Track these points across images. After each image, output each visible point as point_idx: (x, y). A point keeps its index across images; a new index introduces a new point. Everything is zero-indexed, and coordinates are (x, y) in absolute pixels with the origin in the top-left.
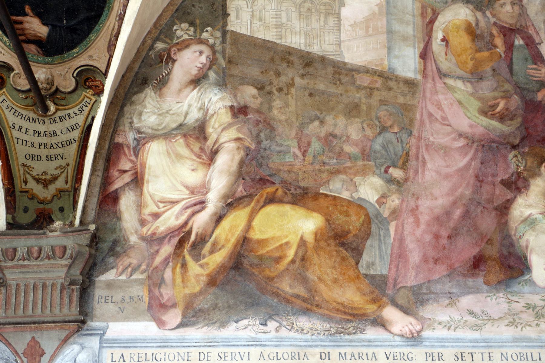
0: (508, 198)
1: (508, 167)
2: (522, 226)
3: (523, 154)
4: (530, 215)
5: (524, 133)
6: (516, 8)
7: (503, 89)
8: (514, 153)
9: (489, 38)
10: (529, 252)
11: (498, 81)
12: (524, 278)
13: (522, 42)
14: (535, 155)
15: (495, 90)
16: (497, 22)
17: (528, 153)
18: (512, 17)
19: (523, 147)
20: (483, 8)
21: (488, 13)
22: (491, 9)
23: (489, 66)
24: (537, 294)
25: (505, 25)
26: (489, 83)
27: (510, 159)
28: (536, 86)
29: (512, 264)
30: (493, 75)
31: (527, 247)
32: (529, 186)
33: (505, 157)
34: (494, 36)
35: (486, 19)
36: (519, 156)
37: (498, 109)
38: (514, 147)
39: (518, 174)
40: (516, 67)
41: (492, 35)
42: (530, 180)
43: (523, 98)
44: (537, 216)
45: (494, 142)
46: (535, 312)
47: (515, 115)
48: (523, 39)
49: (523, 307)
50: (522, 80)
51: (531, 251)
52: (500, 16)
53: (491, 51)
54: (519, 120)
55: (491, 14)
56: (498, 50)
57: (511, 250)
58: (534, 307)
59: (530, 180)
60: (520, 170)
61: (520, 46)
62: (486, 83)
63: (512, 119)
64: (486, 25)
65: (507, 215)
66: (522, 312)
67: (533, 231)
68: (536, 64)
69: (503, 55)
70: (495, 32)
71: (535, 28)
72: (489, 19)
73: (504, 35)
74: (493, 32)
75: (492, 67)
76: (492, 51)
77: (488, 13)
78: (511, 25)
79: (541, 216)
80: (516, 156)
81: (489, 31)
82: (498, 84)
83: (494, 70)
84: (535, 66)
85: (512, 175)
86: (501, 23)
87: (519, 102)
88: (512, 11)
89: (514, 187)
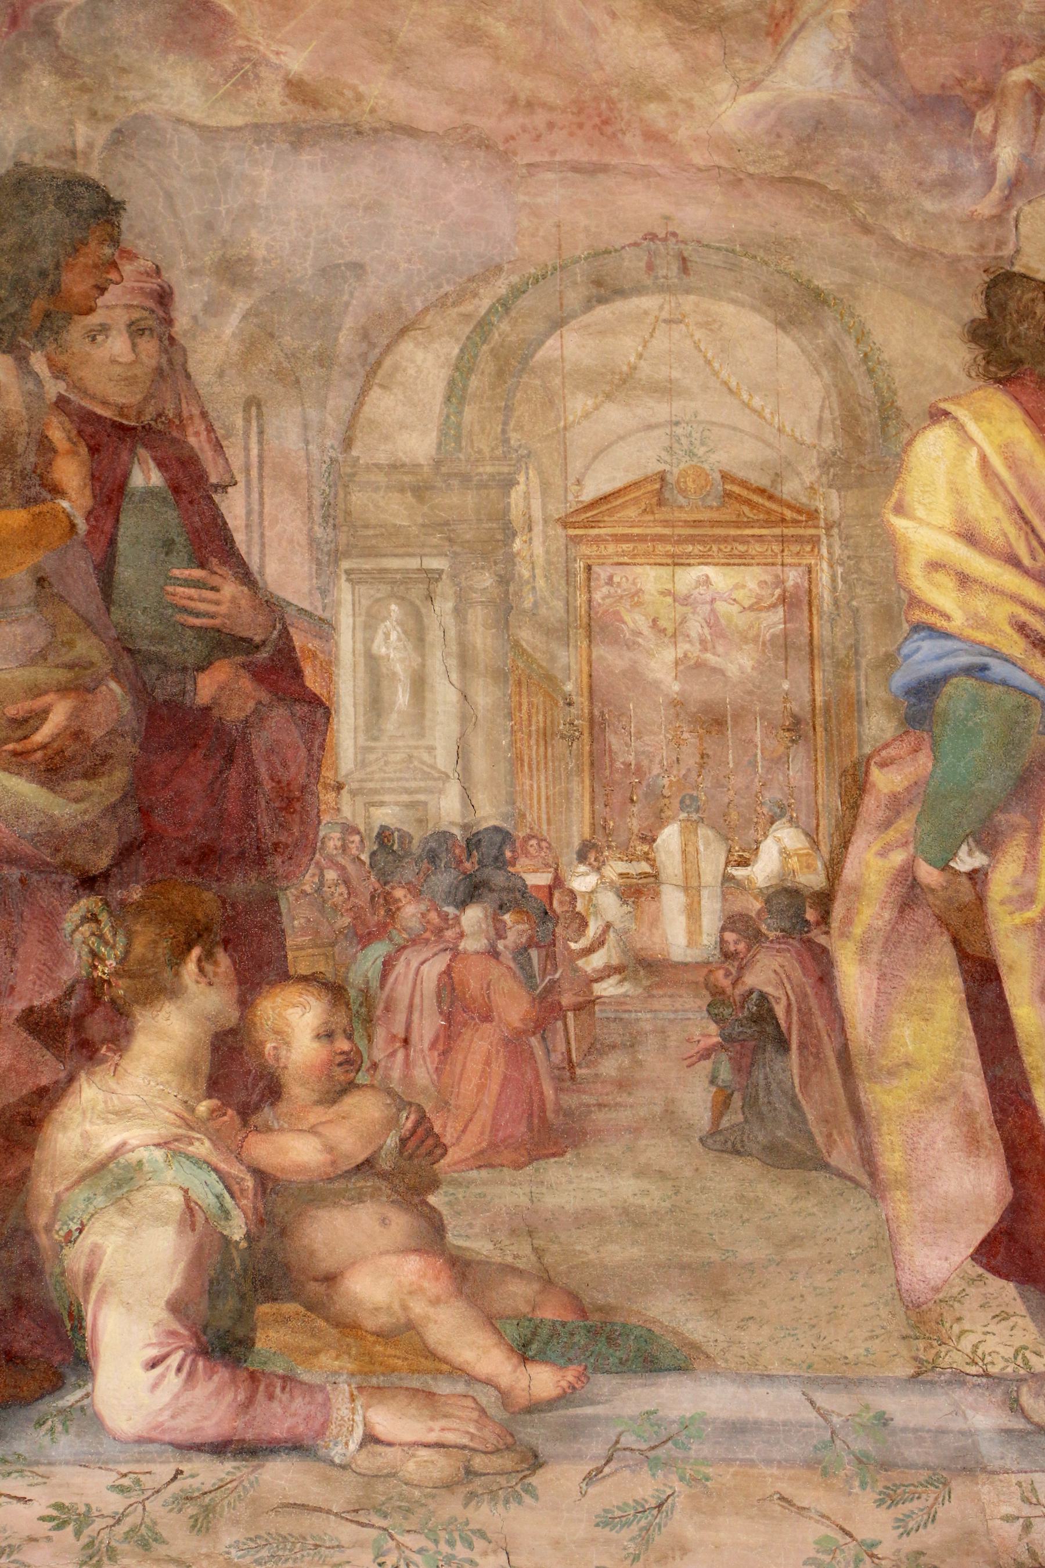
0: (44, 1081)
1: (58, 956)
2: (80, 1194)
3: (121, 912)
4: (120, 1149)
5: (134, 827)
6: (148, 346)
7: (68, 657)
8: (87, 903)
9: (33, 459)
10: (93, 1295)
11: (53, 626)
12: (61, 1403)
13: (156, 478)
14: (168, 916)
15: (42, 655)
16: (72, 397)
17: (140, 908)
18: (130, 381)
19: (123, 885)
20: (23, 341)
21: (38, 362)
22: (51, 347)
23: (24, 567)
24: (104, 1464)
25: (99, 411)
26: (18, 629)
27: (68, 927)
28: (195, 649)
29: (22, 1345)
30: (37, 602)
31: (89, 1277)
32: (129, 1033)
33: (51, 921)
34: (55, 451)
35: (31, 386)
36: (104, 917)
37: (43, 734)
38: (89, 883)
39: (95, 987)
40: (125, 573)
41: (45, 446)
42: (136, 1010)
43: (141, 692)
44: (143, 1154)
45: (11, 862)
46: (84, 1540)
47: (105, 759)
48: (161, 465)
49: (42, 1519)
50: (143, 622)
51: (103, 1292)
52: (82, 374)
53: (36, 509)
54: (120, 776)
55: (51, 364)
56: (65, 504)
57: (25, 1291)
58: (84, 1519)
59: (136, 1010)
60: (102, 971)
61: (151, 493)
62: (7, 629)
63: (90, 774)
64: (28, 409)
65: (29, 1149)
66: (32, 1539)
67: (123, 1212)
68: (202, 566)
69: (82, 526)
70: (57, 436)
71: (210, 429)
72: (39, 383)
73: (94, 450)
74: (50, 434)
75: (37, 568)
76: (44, 508)
77: (38, 362)
78: (121, 410)
79: (159, 1154)
80: (94, 918)
81: (35, 429)
82: (54, 636)
83: (41, 581)
84: (197, 573)
85: (69, 993)
86: (83, 403)
87: (127, 709)
88: (128, 357)
89: (70, 1038)
